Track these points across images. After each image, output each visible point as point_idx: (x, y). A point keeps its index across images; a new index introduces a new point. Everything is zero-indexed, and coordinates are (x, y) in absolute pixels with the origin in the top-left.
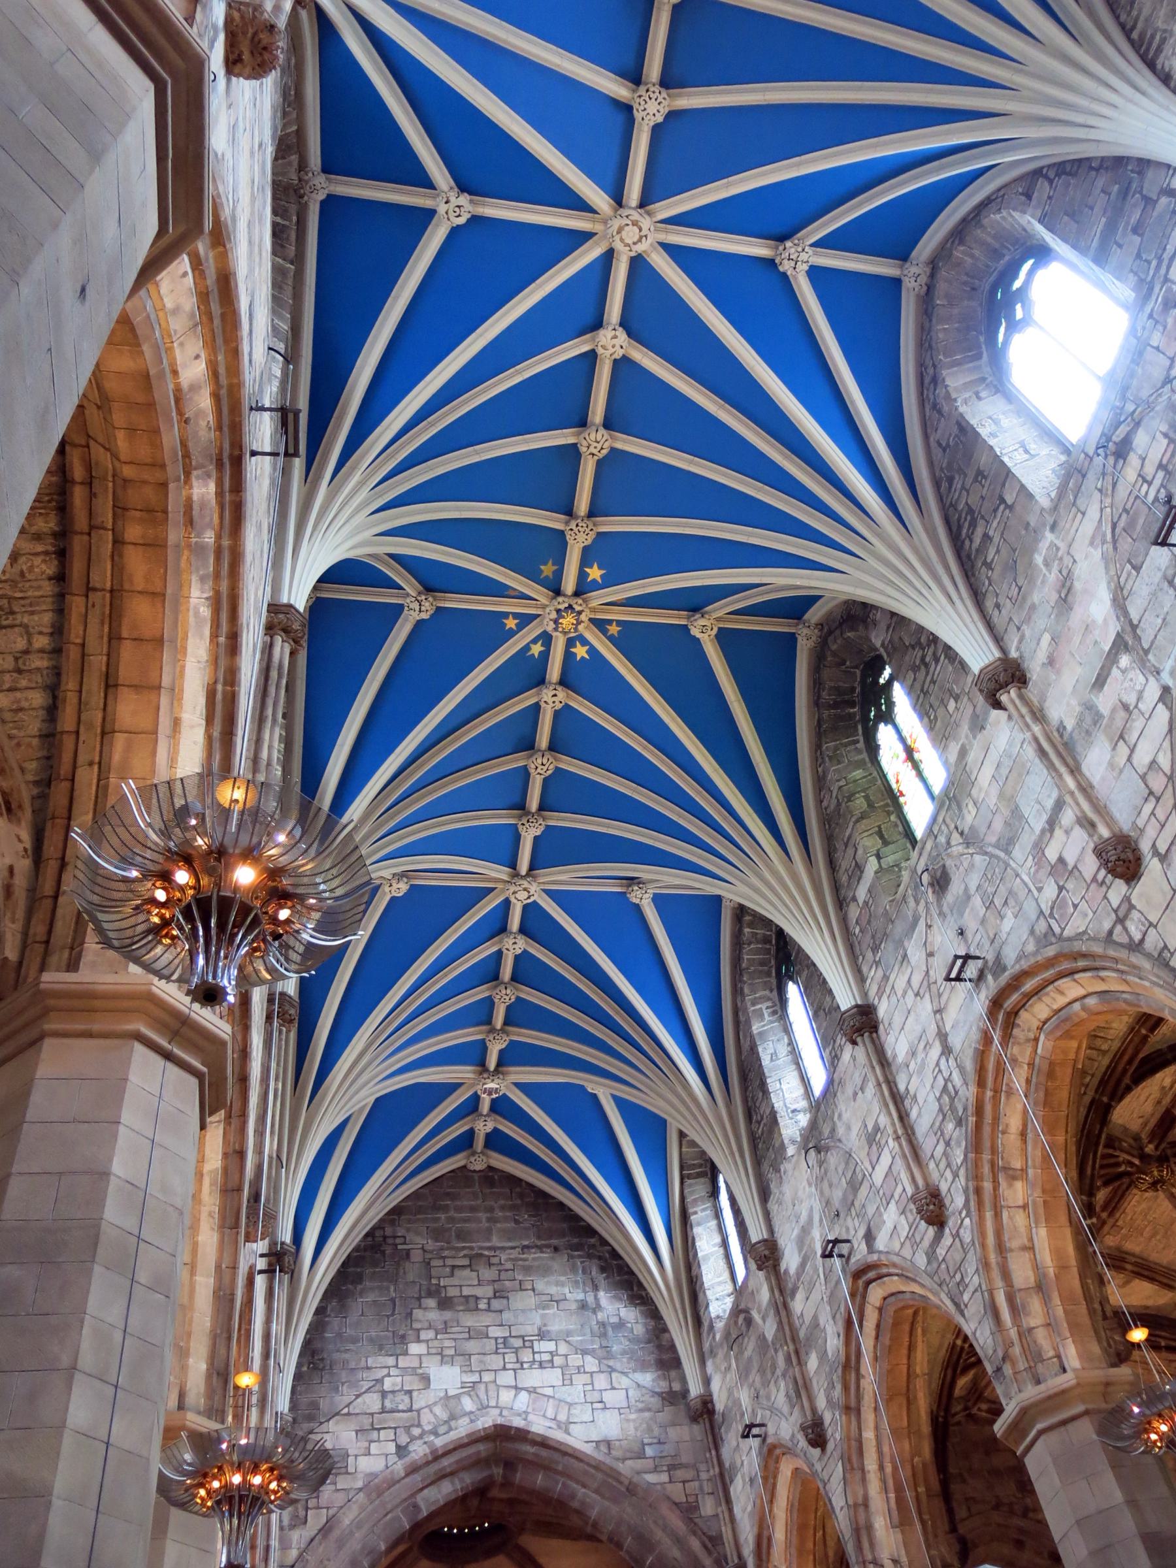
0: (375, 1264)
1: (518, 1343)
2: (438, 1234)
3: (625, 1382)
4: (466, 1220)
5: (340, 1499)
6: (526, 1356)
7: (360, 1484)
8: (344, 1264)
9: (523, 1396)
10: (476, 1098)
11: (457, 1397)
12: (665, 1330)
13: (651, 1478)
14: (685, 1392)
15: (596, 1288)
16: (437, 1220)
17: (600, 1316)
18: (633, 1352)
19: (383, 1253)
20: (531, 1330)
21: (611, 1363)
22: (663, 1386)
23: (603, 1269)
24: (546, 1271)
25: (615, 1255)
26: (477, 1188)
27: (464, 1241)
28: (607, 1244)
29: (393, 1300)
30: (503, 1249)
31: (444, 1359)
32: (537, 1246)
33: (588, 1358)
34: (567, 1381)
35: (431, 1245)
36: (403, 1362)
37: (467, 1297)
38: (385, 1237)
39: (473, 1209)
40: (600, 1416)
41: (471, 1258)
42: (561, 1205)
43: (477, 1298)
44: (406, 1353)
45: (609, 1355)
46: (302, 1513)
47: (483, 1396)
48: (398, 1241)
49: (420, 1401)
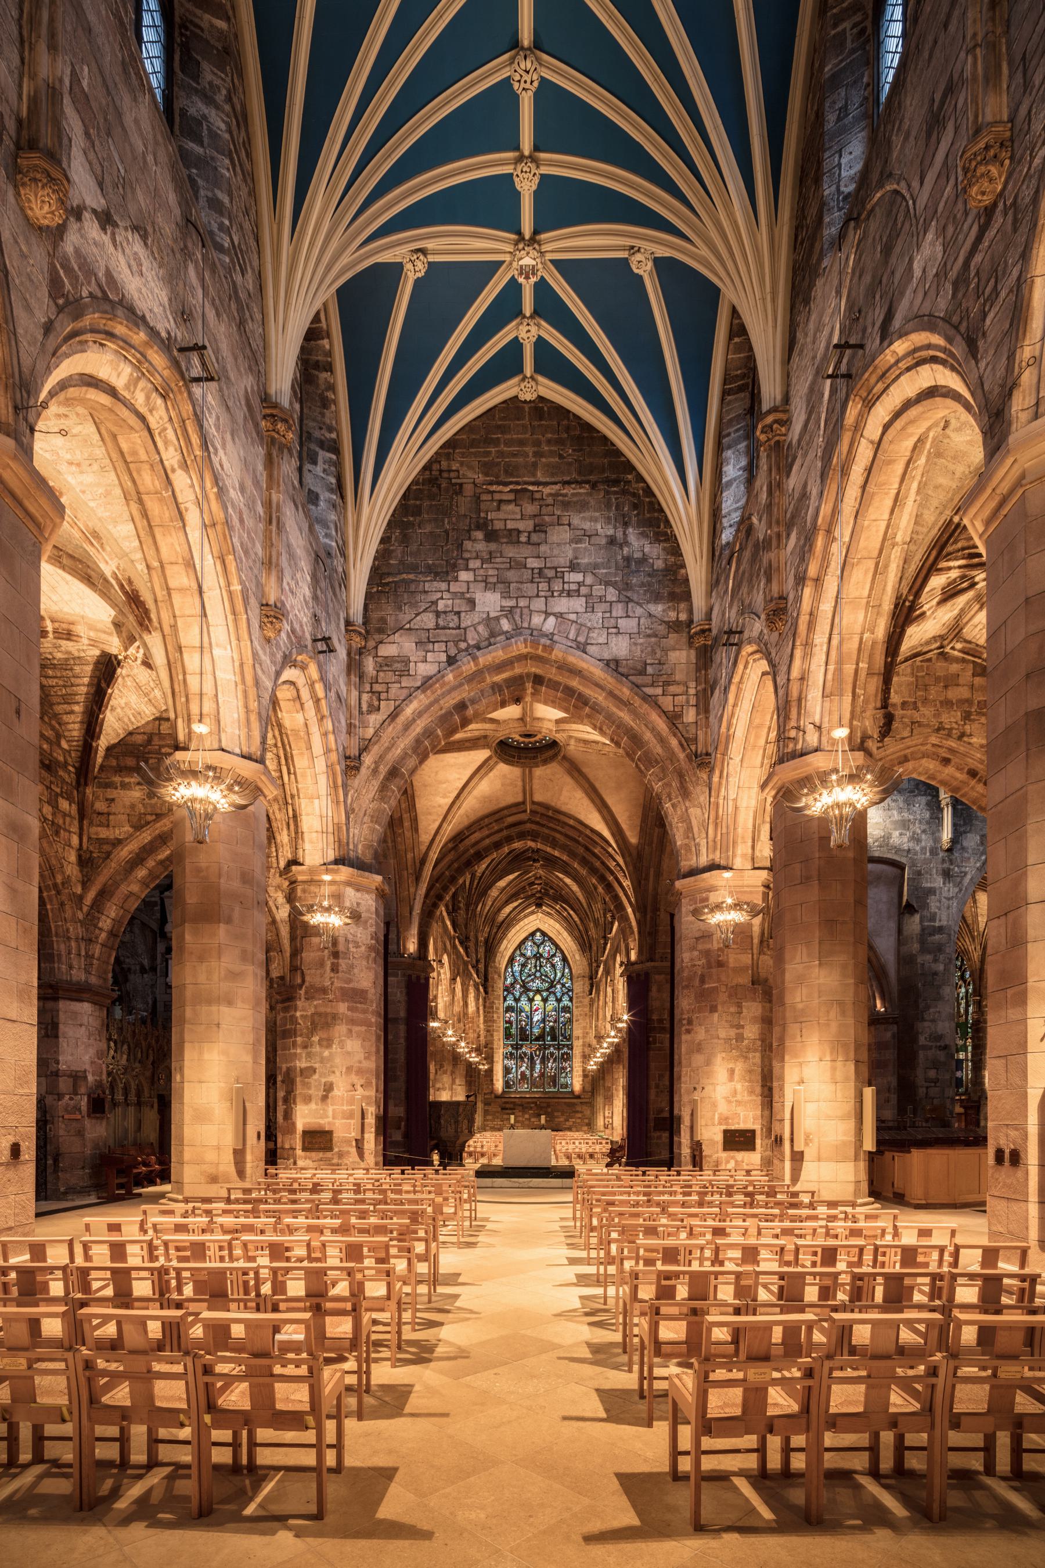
0: (432, 497)
1: (550, 573)
2: (487, 468)
3: (639, 611)
4: (515, 455)
5: (405, 692)
6: (557, 586)
7: (419, 684)
8: (405, 496)
9: (552, 620)
10: (513, 288)
11: (497, 619)
12: (683, 566)
13: (649, 691)
14: (690, 622)
15: (626, 524)
16: (489, 453)
17: (626, 550)
18: (649, 584)
19: (439, 487)
20: (563, 561)
21: (629, 594)
22: (673, 615)
23: (635, 506)
24: (583, 506)
25: (649, 491)
26: (526, 421)
27: (512, 475)
28: (643, 480)
29: (447, 532)
30: (546, 484)
31: (488, 586)
32: (577, 482)
33: (611, 589)
34: (590, 608)
35: (481, 478)
36: (454, 587)
37: (510, 530)
38: (441, 471)
39: (521, 443)
40: (613, 640)
41: (516, 491)
42: (605, 439)
43: (519, 532)
44: (456, 579)
45: (628, 586)
46: (376, 703)
47: (517, 618)
48: (452, 475)
49: (467, 621)
